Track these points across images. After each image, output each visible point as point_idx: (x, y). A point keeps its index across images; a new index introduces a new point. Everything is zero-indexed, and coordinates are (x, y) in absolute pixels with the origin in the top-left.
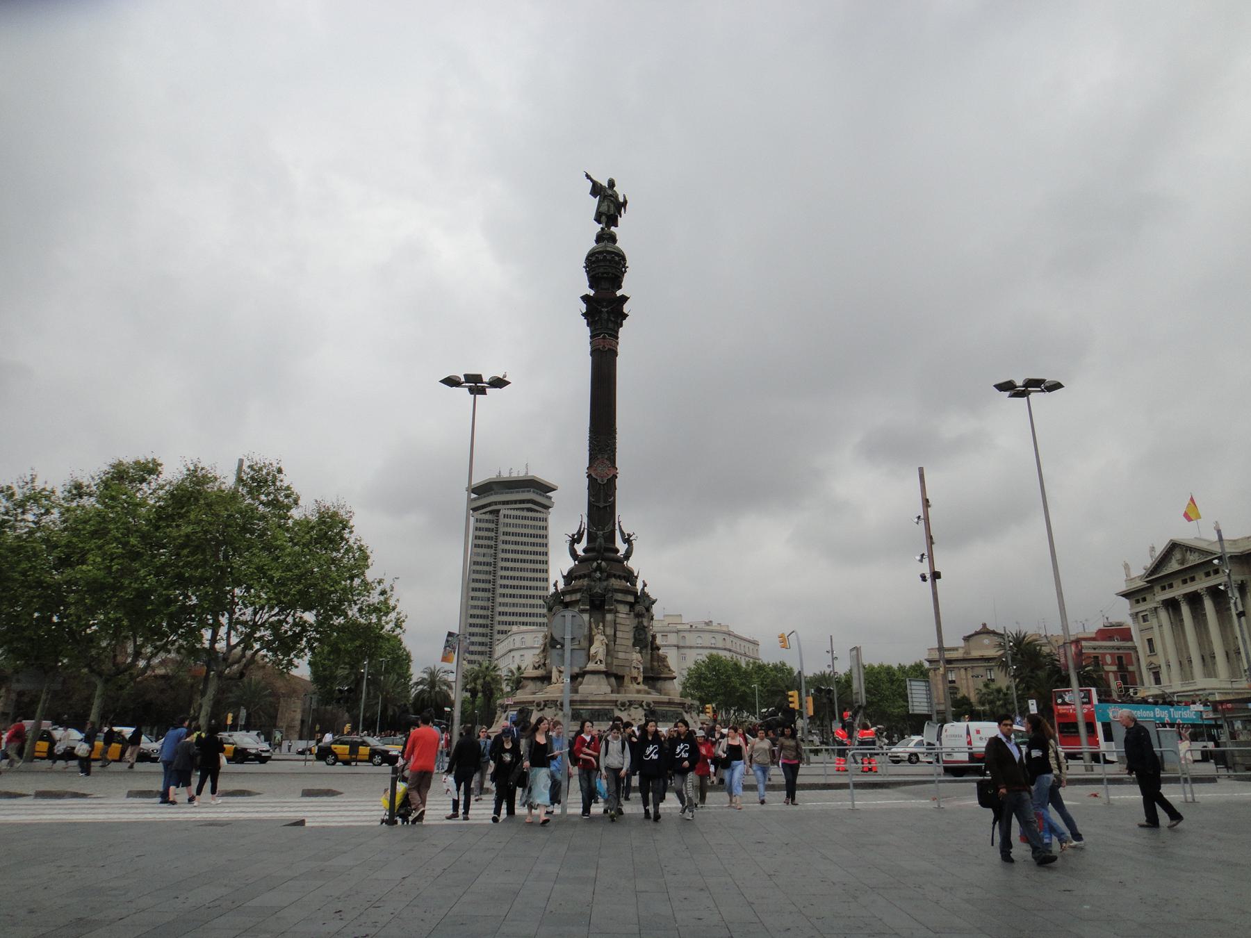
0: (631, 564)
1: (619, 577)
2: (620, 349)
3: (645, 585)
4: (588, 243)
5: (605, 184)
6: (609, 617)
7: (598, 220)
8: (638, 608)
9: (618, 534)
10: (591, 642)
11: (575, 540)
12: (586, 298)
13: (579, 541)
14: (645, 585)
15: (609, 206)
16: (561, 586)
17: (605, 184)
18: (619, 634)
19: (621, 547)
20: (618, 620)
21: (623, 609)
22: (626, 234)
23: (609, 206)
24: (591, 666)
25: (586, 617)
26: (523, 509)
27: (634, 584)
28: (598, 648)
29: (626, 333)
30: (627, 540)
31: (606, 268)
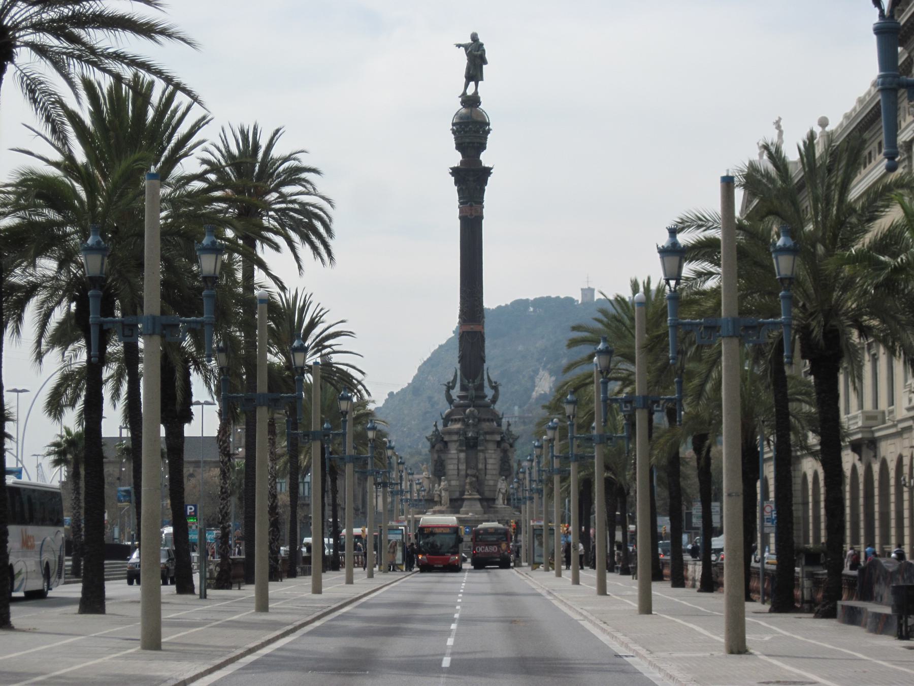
0: (498, 407)
1: (488, 420)
2: (485, 212)
3: (509, 425)
5: (469, 41)
8: (506, 445)
9: (486, 383)
11: (450, 387)
13: (453, 387)
14: (509, 425)
16: (440, 428)
18: (489, 467)
19: (489, 392)
20: (487, 455)
21: (492, 446)
22: (488, 91)
27: (499, 425)
30: (495, 388)
31: (471, 131)
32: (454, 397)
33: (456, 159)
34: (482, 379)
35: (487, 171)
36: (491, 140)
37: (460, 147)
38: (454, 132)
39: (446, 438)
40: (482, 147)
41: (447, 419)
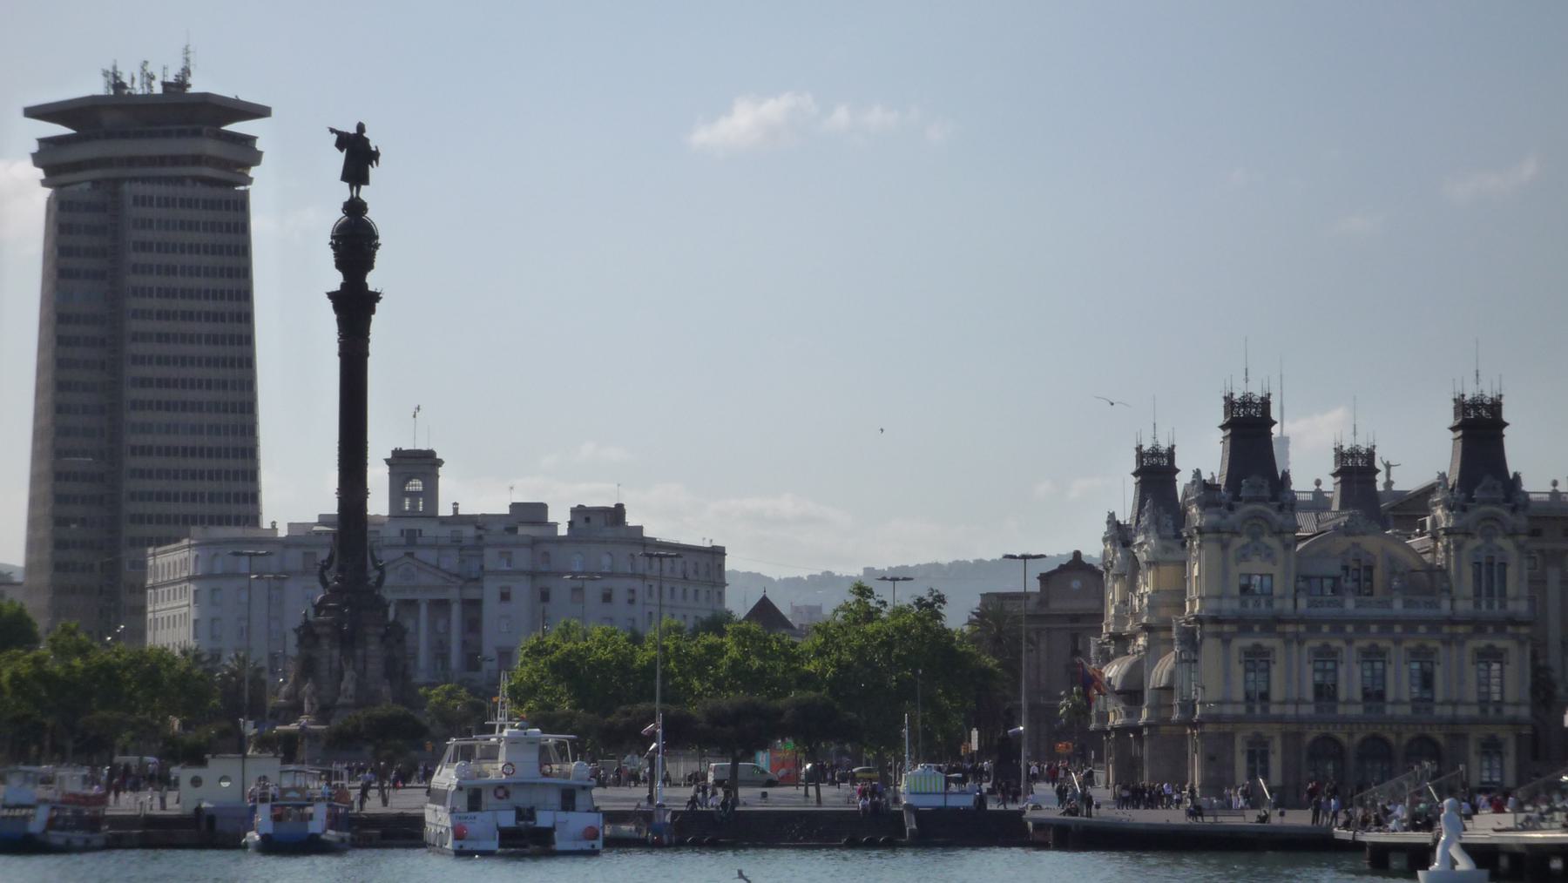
4: (336, 215)
5: (353, 130)
6: (359, 652)
7: (345, 178)
10: (341, 679)
12: (332, 295)
13: (327, 568)
15: (358, 156)
17: (353, 130)
19: (373, 575)
23: (358, 156)
24: (341, 700)
25: (336, 653)
26: (180, 180)
28: (348, 685)
29: (380, 325)
32: (329, 579)
33: (336, 280)
34: (365, 558)
35: (375, 297)
36: (380, 257)
37: (340, 265)
38: (334, 247)
39: (318, 630)
40: (369, 265)
41: (318, 608)
